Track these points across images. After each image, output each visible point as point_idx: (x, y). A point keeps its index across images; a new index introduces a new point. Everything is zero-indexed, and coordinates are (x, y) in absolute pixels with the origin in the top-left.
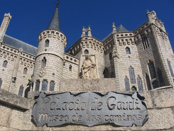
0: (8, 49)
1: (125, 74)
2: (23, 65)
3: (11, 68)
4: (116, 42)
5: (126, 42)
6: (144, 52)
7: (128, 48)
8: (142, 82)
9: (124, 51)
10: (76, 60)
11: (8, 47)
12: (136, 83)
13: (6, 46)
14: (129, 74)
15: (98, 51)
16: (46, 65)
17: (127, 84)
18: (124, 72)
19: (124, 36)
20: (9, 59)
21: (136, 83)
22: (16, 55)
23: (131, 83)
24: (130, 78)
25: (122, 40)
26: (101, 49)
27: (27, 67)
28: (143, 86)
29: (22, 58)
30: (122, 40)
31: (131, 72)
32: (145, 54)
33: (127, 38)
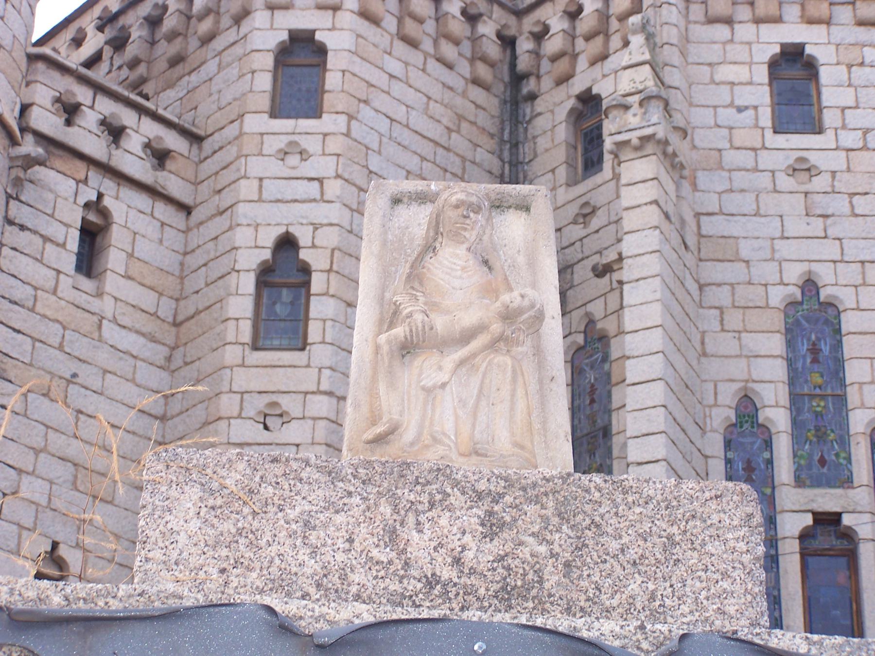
1: (737, 369)
9: (745, 96)
10: (172, 141)
14: (778, 370)
15: (440, 60)
18: (725, 344)
23: (799, 482)
24: (796, 401)
26: (475, 39)
31: (815, 350)
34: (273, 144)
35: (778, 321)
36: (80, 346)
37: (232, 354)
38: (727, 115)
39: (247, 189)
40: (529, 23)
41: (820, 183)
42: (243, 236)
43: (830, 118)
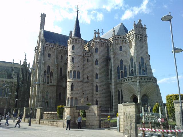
0: (49, 45)
2: (60, 54)
7: (121, 47)
11: (49, 44)
12: (123, 69)
13: (48, 44)
16: (74, 62)
19: (119, 38)
21: (123, 69)
23: (121, 69)
24: (120, 66)
25: (118, 41)
27: (62, 55)
30: (118, 41)
33: (121, 40)
35: (119, 61)
36: (88, 66)
42: (94, 59)
43: (122, 50)
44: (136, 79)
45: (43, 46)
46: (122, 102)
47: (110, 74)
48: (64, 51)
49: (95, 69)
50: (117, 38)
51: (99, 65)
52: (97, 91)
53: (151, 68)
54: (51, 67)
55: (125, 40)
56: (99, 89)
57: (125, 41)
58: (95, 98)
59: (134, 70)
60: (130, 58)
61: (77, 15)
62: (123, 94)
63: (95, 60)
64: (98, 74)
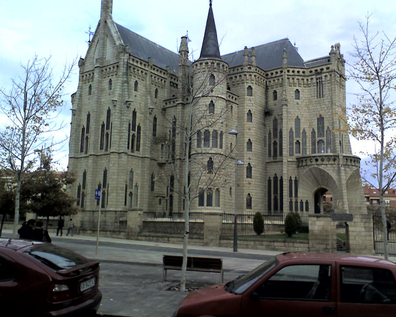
0: (137, 62)
2: (154, 86)
3: (142, 92)
4: (286, 81)
5: (297, 83)
6: (317, 102)
7: (297, 91)
8: (307, 137)
10: (237, 97)
11: (136, 59)
12: (300, 137)
13: (134, 58)
14: (294, 126)
17: (291, 137)
19: (296, 73)
20: (139, 79)
21: (300, 137)
22: (147, 71)
23: (296, 137)
24: (295, 129)
25: (293, 79)
27: (157, 87)
28: (307, 142)
29: (153, 75)
30: (293, 79)
32: (316, 105)
33: (299, 77)
34: (248, 99)
37: (245, 123)
38: (291, 97)
39: (246, 104)
40: (268, 80)
41: (299, 106)
42: (245, 110)
43: (300, 98)
44: (337, 159)
45: (126, 63)
46: (296, 200)
47: (267, 143)
48: (161, 80)
49: (247, 131)
50: (291, 73)
51: (254, 123)
52: (249, 175)
53: (349, 141)
54: (138, 114)
55: (307, 80)
56: (253, 172)
57: (308, 82)
58: (245, 191)
59: (325, 141)
60: (316, 118)
61: (211, 5)
62: (300, 186)
63: (247, 112)
64: (253, 142)
